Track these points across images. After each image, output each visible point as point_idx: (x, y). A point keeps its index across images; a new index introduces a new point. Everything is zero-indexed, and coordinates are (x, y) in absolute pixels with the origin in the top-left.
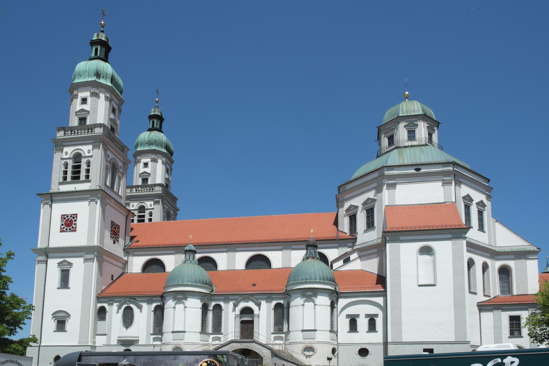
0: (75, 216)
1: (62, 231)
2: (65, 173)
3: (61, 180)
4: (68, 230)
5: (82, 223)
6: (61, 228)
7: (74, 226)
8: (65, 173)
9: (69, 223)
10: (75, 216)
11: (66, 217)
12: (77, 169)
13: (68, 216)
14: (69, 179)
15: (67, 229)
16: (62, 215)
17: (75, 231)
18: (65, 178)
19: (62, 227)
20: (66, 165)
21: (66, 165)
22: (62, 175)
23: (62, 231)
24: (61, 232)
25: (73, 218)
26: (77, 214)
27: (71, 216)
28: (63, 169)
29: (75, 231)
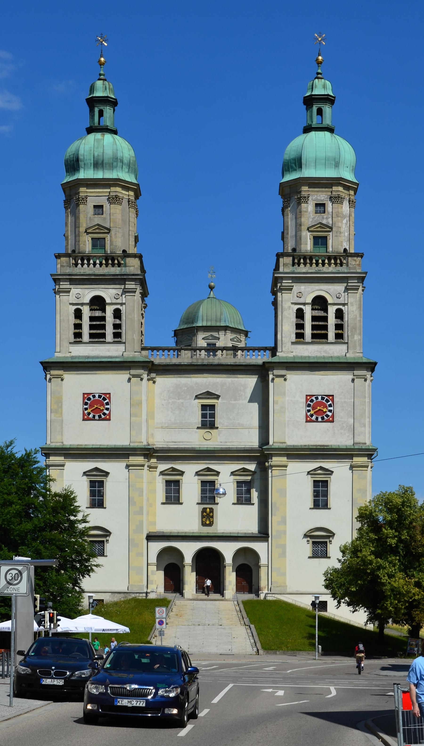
0: (105, 397)
2: (78, 326)
3: (72, 339)
4: (97, 417)
6: (84, 414)
7: (107, 412)
8: (78, 326)
9: (96, 407)
10: (105, 397)
11: (91, 397)
12: (97, 325)
13: (94, 396)
14: (86, 337)
15: (94, 416)
16: (84, 394)
17: (109, 420)
20: (78, 314)
21: (78, 314)
22: (72, 330)
25: (104, 399)
27: (100, 397)
28: (72, 320)
29: (109, 420)
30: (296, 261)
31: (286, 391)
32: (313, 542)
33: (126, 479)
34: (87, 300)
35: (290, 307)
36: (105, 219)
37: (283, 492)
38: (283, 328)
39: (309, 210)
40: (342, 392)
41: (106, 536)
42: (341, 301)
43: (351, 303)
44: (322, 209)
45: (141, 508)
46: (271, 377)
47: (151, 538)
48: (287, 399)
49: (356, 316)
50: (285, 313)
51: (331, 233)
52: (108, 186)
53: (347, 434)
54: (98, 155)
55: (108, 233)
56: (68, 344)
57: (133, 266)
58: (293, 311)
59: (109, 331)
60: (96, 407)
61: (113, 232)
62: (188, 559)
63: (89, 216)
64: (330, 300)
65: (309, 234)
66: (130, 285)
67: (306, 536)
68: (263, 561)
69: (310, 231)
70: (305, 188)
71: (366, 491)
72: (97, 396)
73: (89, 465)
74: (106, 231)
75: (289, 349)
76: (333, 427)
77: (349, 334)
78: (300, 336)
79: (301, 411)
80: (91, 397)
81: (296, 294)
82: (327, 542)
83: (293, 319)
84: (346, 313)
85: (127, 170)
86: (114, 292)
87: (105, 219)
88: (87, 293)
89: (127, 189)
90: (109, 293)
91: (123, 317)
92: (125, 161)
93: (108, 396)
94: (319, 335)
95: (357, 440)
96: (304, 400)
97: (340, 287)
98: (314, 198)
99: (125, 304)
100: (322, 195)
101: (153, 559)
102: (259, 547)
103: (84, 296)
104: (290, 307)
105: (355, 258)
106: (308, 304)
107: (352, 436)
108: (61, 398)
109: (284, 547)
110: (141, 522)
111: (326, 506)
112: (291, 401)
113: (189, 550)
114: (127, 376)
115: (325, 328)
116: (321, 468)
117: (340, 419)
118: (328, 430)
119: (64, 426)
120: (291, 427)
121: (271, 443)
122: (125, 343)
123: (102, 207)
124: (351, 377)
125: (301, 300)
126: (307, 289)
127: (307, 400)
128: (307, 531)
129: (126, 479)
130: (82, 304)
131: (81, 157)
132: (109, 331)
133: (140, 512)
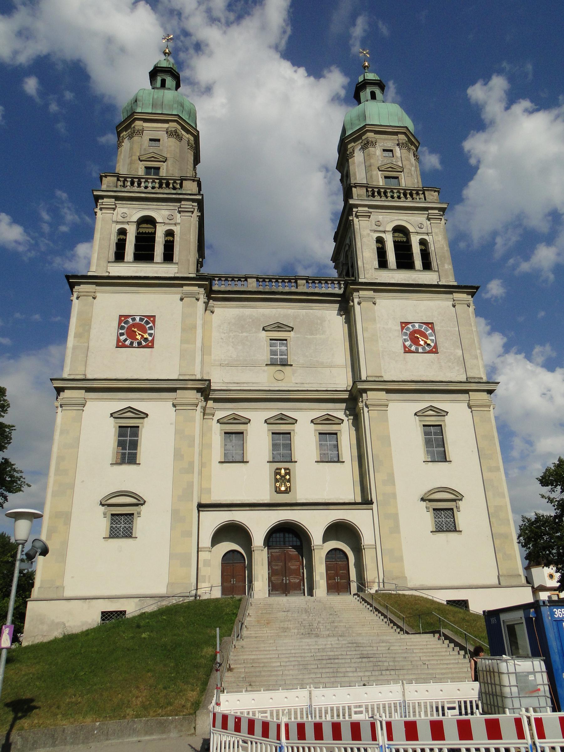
1: (120, 345)
3: (112, 257)
5: (166, 333)
6: (118, 340)
9: (135, 332)
11: (130, 320)
13: (134, 319)
15: (132, 343)
17: (152, 347)
18: (119, 256)
19: (122, 338)
20: (122, 232)
21: (122, 232)
22: (113, 249)
23: (120, 345)
24: (118, 346)
25: (147, 323)
26: (154, 317)
27: (141, 320)
28: (114, 239)
29: (152, 347)
30: (370, 194)
31: (377, 318)
32: (434, 509)
33: (171, 424)
34: (135, 218)
35: (369, 234)
36: (161, 150)
37: (386, 440)
38: (364, 254)
39: (377, 154)
40: (443, 320)
41: (136, 505)
42: (424, 230)
43: (435, 233)
44: (390, 154)
45: (191, 464)
46: (356, 301)
47: (201, 507)
48: (378, 325)
49: (443, 245)
50: (364, 240)
51: (402, 174)
52: (167, 121)
53: (457, 368)
54: (158, 97)
55: (164, 162)
56: (105, 264)
57: (190, 187)
58: (372, 238)
59: (158, 251)
60: (135, 332)
61: (169, 162)
62: (258, 539)
63: (144, 147)
64: (411, 229)
65: (380, 173)
66: (186, 205)
67: (423, 499)
68: (367, 539)
69: (380, 171)
70: (370, 135)
71: (494, 437)
72: (138, 319)
73: (118, 403)
74: (162, 159)
75: (372, 275)
76: (438, 359)
77: (439, 263)
78: (383, 264)
79: (397, 341)
80: (130, 320)
81: (374, 222)
82: (452, 509)
83: (374, 246)
84: (432, 243)
85: (188, 117)
86: (167, 213)
87: (161, 150)
88: (135, 212)
89: (188, 132)
90: (160, 213)
91: (177, 239)
92: (186, 108)
93: (152, 319)
94: (405, 261)
95: (470, 374)
96: (400, 328)
97: (421, 218)
98: (381, 145)
99: (179, 223)
100: (389, 142)
101: (206, 541)
102: (360, 519)
103: (131, 216)
104: (369, 234)
105: (433, 193)
106: (389, 231)
107: (463, 370)
108: (90, 320)
109: (395, 517)
110: (190, 485)
111: (443, 458)
112: (384, 328)
113: (259, 525)
114: (179, 296)
115: (411, 255)
116: (432, 408)
117: (445, 350)
118: (432, 362)
119: (89, 354)
120: (388, 359)
121: (364, 378)
122: (177, 263)
123: (159, 140)
124: (451, 303)
125: (381, 229)
126: (386, 219)
127: (402, 328)
128: (423, 493)
129: (171, 424)
130: (128, 223)
131: (139, 98)
132: (158, 251)
133: (190, 469)
